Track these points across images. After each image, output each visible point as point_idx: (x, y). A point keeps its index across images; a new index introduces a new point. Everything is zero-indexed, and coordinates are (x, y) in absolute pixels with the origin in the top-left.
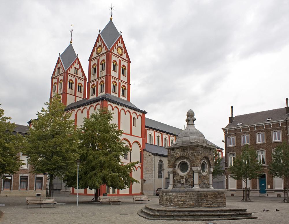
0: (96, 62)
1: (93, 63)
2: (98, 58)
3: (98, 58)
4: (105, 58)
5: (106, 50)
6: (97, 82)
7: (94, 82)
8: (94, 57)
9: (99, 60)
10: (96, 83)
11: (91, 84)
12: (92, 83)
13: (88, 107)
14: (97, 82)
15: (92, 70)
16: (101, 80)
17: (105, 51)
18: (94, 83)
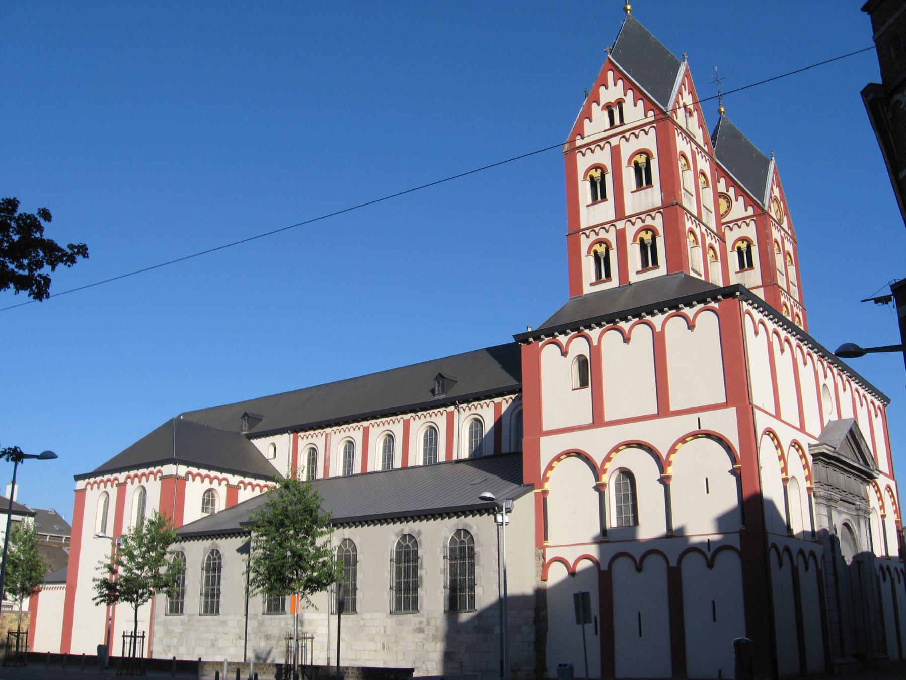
0: (603, 157)
5: (651, 114)
6: (621, 234)
9: (615, 152)
10: (611, 237)
12: (593, 237)
13: (657, 320)
14: (621, 234)
16: (639, 224)
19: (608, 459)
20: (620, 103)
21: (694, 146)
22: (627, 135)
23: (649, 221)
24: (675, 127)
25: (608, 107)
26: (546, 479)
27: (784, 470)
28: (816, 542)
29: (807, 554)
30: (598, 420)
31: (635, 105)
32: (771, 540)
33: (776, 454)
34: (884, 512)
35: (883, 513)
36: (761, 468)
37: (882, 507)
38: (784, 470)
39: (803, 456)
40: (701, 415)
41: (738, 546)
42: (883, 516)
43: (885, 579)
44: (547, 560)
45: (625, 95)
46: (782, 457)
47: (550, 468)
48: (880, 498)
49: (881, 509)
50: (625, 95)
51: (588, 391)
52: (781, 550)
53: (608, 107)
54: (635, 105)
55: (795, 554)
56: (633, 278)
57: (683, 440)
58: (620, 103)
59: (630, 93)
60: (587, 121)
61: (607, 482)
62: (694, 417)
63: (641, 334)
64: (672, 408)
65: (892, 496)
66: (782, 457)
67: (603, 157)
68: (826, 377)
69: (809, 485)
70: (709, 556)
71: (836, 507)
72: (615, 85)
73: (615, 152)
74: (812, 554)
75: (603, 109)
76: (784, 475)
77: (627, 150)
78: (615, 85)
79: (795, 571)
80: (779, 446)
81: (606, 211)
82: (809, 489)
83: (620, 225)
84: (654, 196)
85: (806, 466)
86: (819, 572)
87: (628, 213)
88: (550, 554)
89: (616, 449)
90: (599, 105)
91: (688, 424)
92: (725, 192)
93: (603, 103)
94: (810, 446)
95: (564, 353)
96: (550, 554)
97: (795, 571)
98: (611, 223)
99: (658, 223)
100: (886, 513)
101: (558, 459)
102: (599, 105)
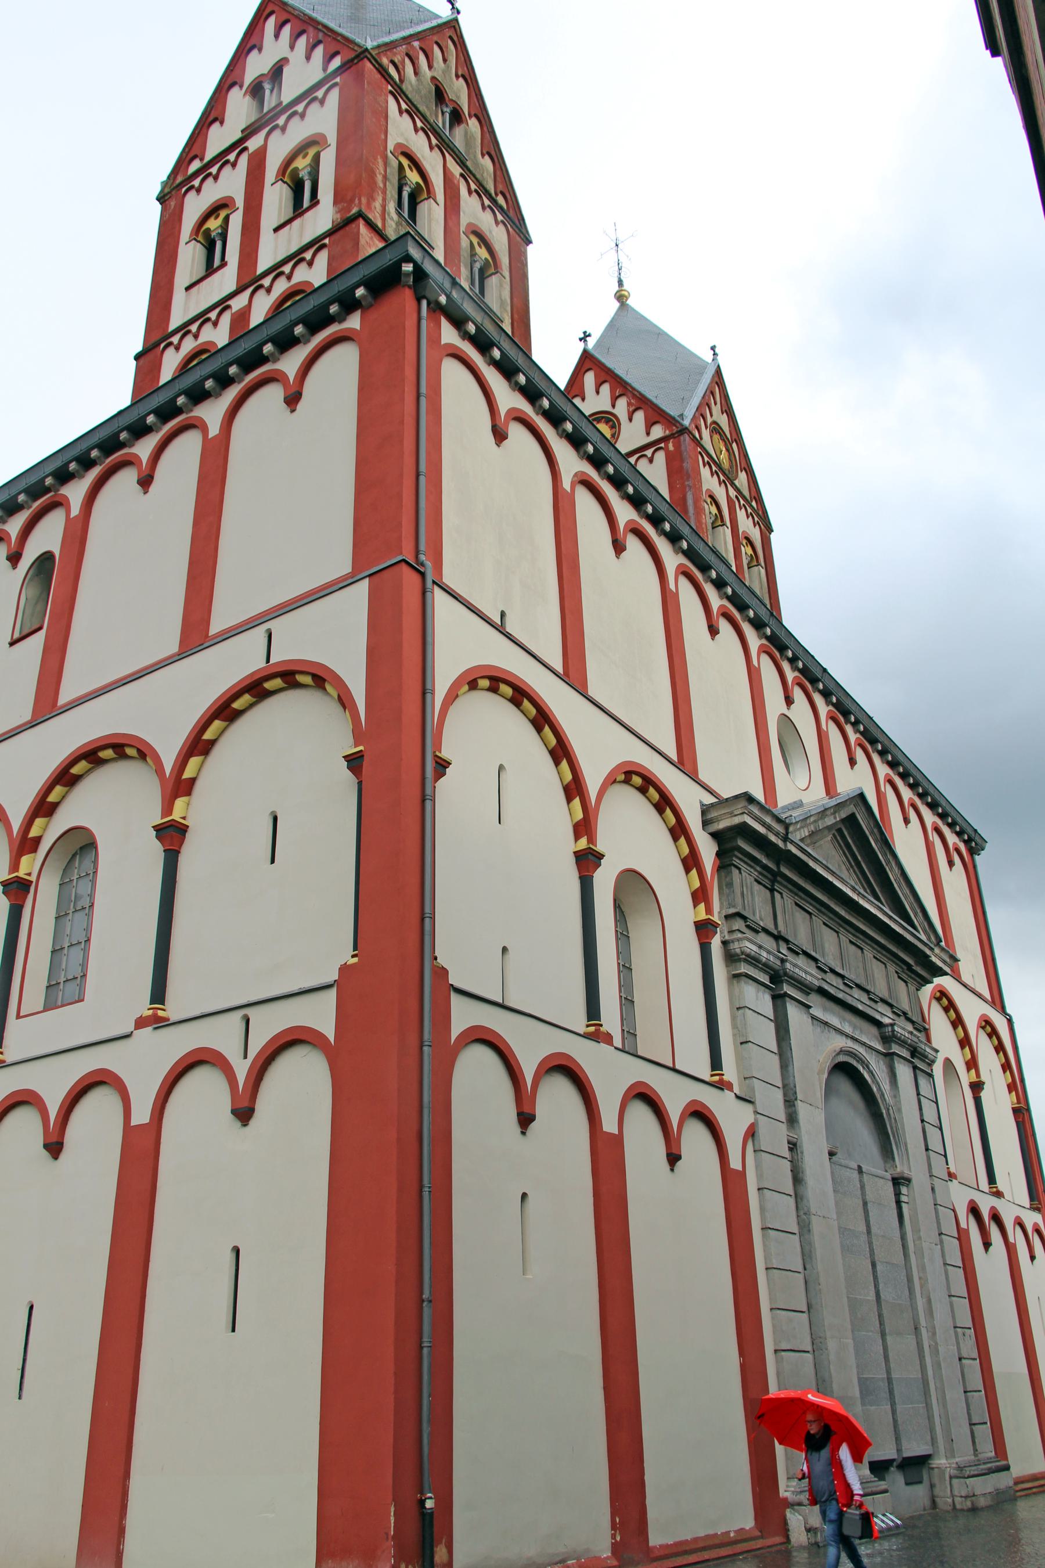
1: (194, 207)
19: (43, 808)
21: (456, 170)
22: (281, 121)
24: (390, 88)
31: (308, 58)
34: (978, 1075)
35: (974, 1079)
36: (442, 766)
37: (972, 1064)
39: (679, 830)
42: (977, 1087)
43: (987, 1245)
45: (292, 47)
48: (965, 1042)
49: (968, 1070)
50: (292, 47)
53: (256, 91)
54: (308, 58)
58: (277, 72)
61: (33, 878)
65: (1000, 1048)
68: (789, 701)
69: (702, 915)
70: (242, 1069)
71: (808, 1007)
72: (277, 36)
75: (245, 94)
76: (583, 843)
78: (277, 36)
82: (704, 929)
85: (691, 862)
90: (241, 87)
94: (705, 810)
98: (223, 305)
100: (983, 1078)
102: (241, 87)
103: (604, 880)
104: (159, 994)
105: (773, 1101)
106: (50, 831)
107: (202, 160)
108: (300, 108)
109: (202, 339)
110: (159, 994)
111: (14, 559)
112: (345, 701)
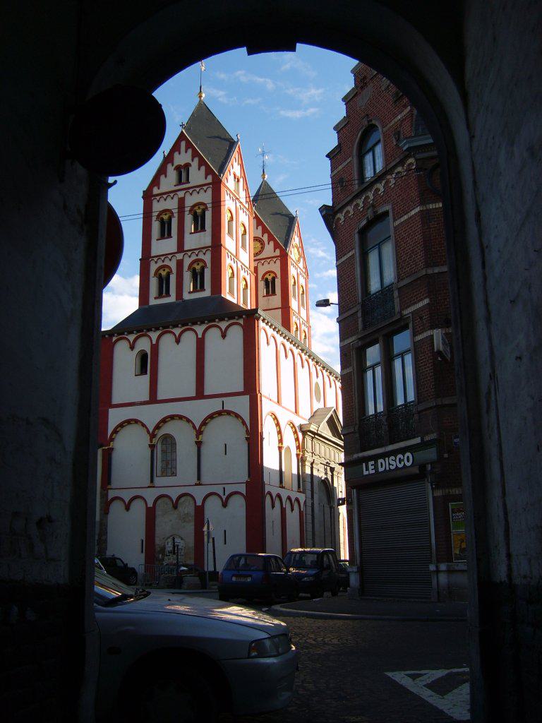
0: (172, 204)
1: (157, 207)
2: (181, 194)
3: (181, 194)
4: (206, 197)
6: (180, 264)
7: (167, 260)
8: (159, 192)
9: (182, 202)
10: (173, 265)
11: (153, 267)
12: (160, 263)
14: (180, 264)
15: (156, 226)
16: (194, 257)
17: (206, 178)
18: (167, 262)
19: (158, 427)
20: (187, 166)
21: (238, 204)
23: (201, 256)
25: (178, 168)
26: (112, 439)
27: (281, 441)
28: (300, 492)
29: (293, 500)
30: (153, 399)
32: (267, 489)
33: (275, 430)
38: (281, 441)
39: (295, 432)
40: (225, 399)
41: (244, 493)
44: (110, 498)
45: (193, 160)
46: (279, 432)
47: (115, 431)
50: (193, 160)
51: (146, 378)
52: (274, 496)
53: (178, 168)
55: (284, 500)
56: (186, 296)
57: (211, 417)
58: (187, 166)
59: (196, 160)
60: (162, 177)
62: (219, 400)
63: (189, 339)
64: (207, 393)
66: (279, 432)
67: (172, 204)
70: (224, 498)
72: (186, 152)
73: (182, 202)
74: (297, 500)
77: (190, 201)
78: (186, 152)
79: (283, 511)
80: (278, 424)
81: (170, 245)
83: (179, 256)
84: (205, 239)
85: (297, 439)
86: (301, 513)
87: (186, 248)
88: (111, 494)
89: (164, 421)
91: (215, 405)
92: (260, 236)
93: (176, 164)
95: (132, 348)
96: (111, 494)
97: (283, 511)
99: (207, 258)
101: (121, 425)
103: (283, 452)
104: (199, 478)
105: (309, 493)
106: (161, 433)
107: (159, 188)
108: (198, 189)
109: (164, 263)
110: (199, 478)
111: (132, 348)
112: (244, 423)
